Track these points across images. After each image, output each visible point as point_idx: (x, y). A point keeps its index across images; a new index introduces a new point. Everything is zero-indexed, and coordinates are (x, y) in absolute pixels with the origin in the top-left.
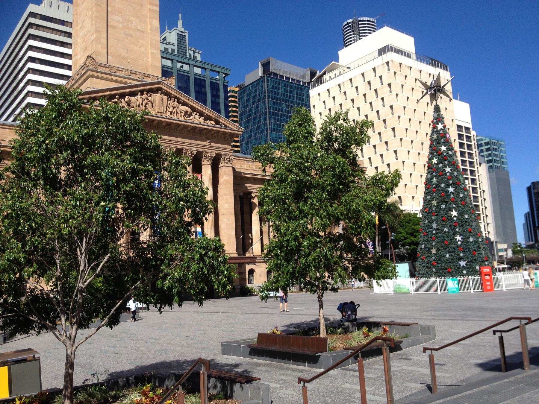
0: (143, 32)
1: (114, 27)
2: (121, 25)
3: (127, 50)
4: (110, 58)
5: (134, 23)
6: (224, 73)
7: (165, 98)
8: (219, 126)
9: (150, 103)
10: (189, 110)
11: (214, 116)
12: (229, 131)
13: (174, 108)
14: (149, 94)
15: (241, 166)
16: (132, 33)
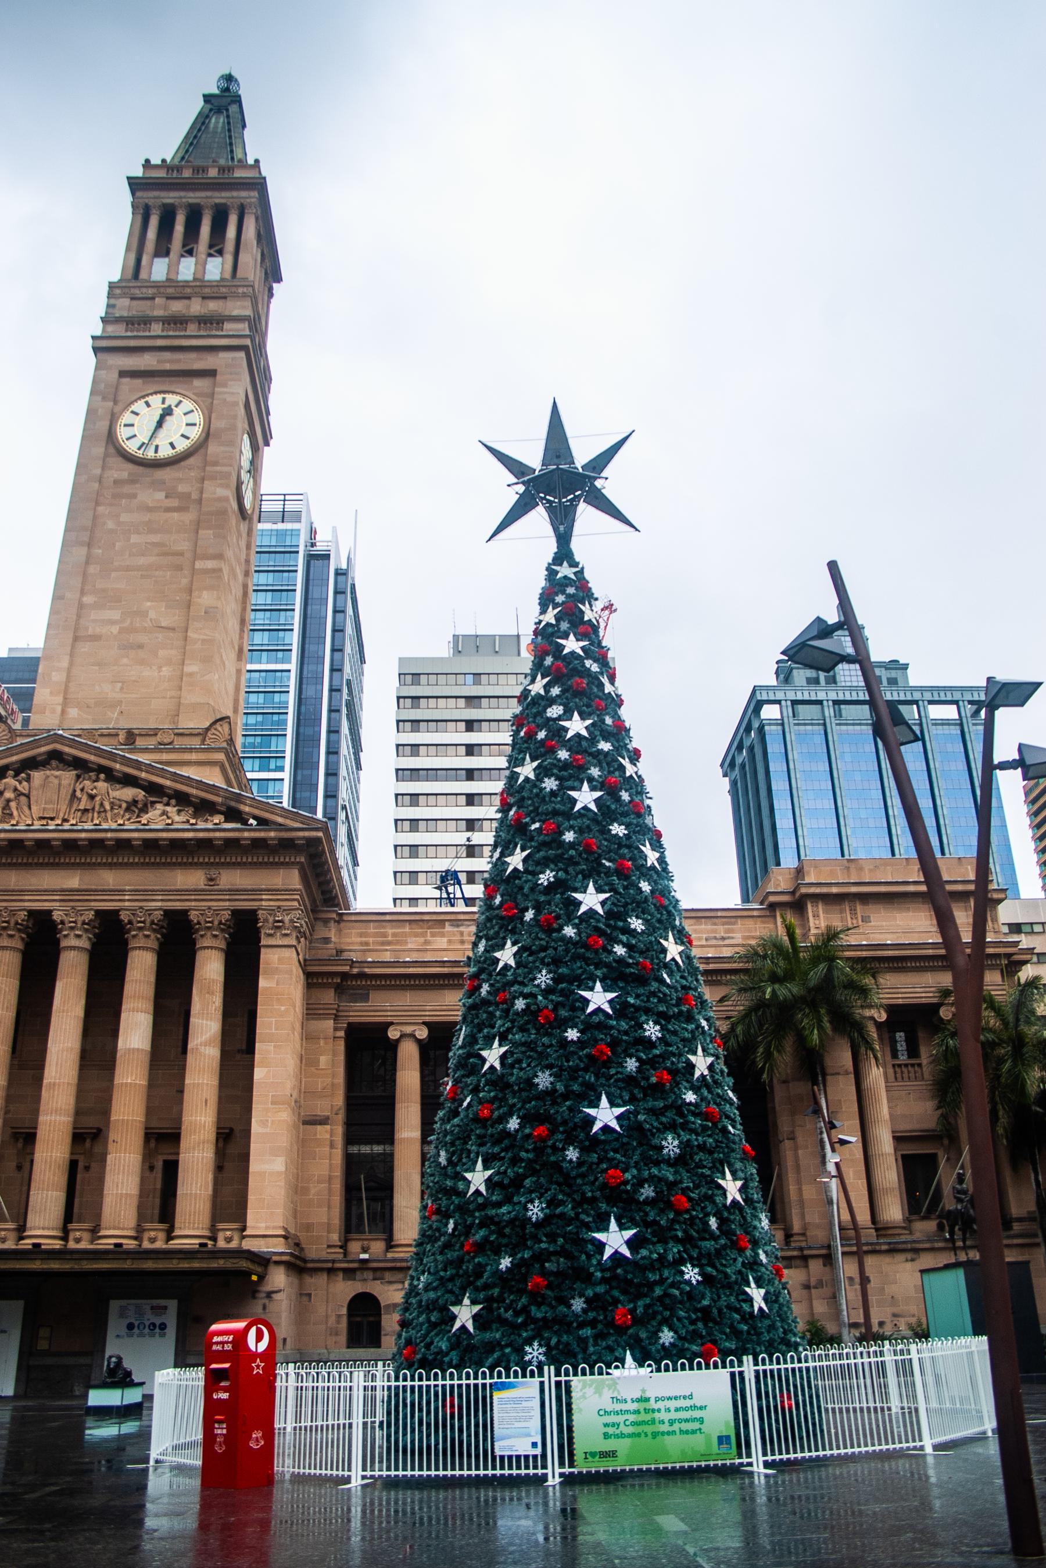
0: (173, 629)
1: (96, 638)
2: (115, 629)
3: (123, 682)
4: (73, 712)
5: (152, 614)
6: (970, 702)
7: (68, 776)
8: (239, 826)
9: (23, 799)
10: (140, 794)
11: (220, 800)
12: (272, 834)
13: (92, 797)
14: (23, 775)
15: (426, 942)
16: (142, 638)
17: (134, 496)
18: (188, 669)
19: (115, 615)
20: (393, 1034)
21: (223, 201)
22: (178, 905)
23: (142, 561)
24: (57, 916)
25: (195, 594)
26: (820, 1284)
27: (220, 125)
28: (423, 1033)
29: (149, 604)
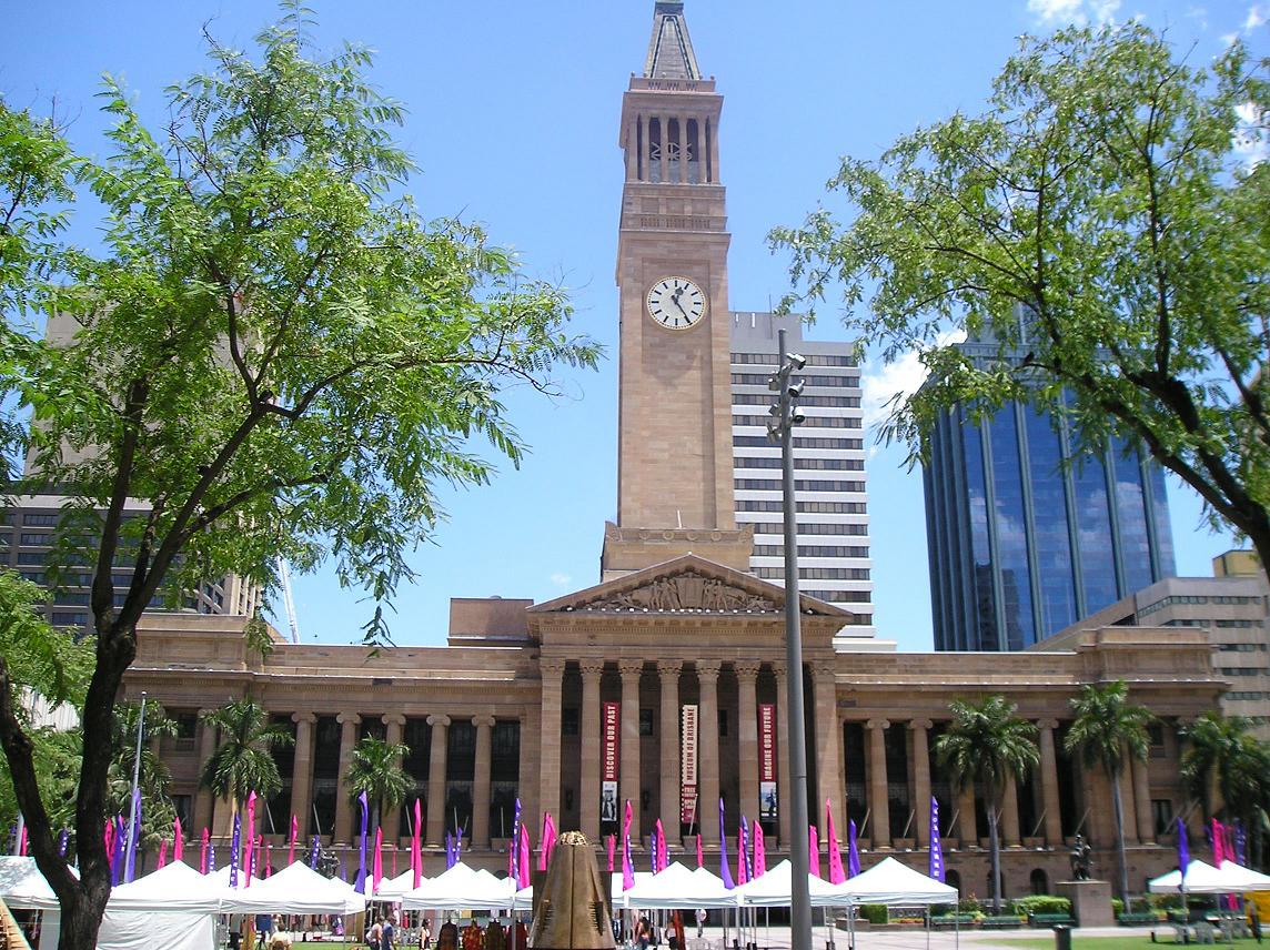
1: (654, 461)
2: (666, 455)
5: (688, 444)
7: (699, 581)
10: (743, 595)
14: (672, 581)
17: (664, 357)
18: (718, 486)
19: (665, 445)
20: (870, 725)
21: (694, 113)
22: (767, 659)
23: (675, 406)
24: (700, 663)
25: (716, 433)
26: (1107, 870)
27: (674, 32)
28: (887, 725)
29: (686, 438)
